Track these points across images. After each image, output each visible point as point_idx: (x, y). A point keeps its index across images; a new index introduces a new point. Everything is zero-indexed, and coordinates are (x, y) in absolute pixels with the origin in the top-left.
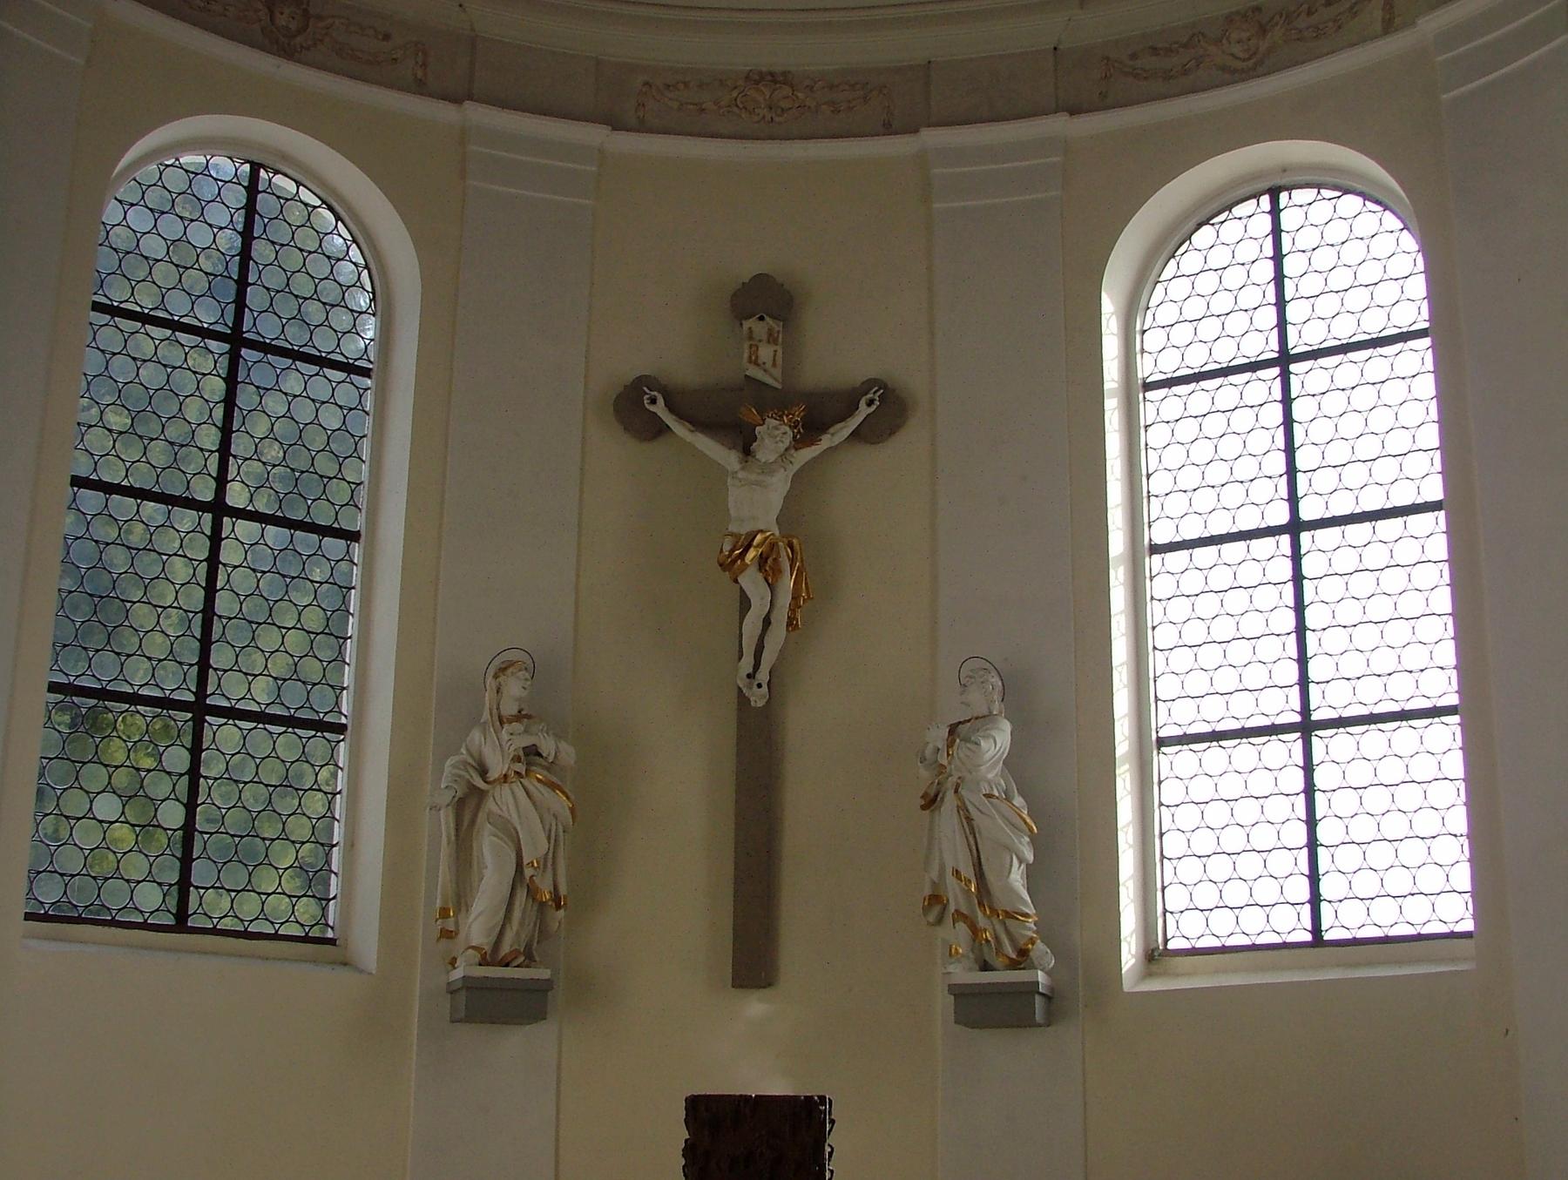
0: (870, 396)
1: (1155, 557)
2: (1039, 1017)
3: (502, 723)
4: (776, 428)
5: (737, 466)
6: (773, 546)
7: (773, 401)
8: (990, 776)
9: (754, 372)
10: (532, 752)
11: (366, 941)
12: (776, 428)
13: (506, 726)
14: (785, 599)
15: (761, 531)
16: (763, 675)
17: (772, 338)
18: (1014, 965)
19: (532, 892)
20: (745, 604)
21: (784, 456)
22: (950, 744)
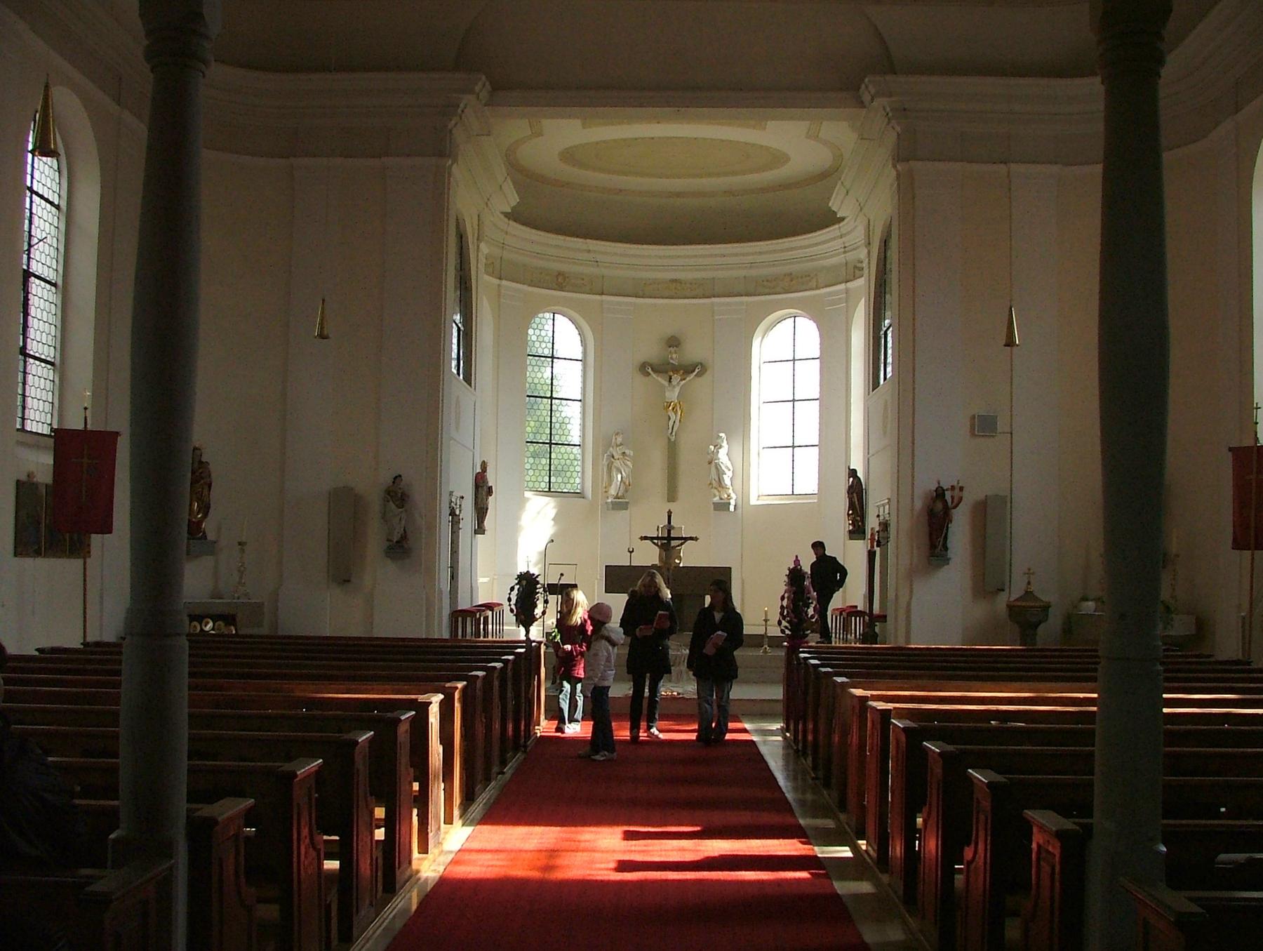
6: (676, 405)
7: (675, 369)
9: (671, 361)
10: (624, 453)
11: (589, 492)
16: (674, 434)
17: (676, 353)
19: (625, 483)
21: (678, 383)
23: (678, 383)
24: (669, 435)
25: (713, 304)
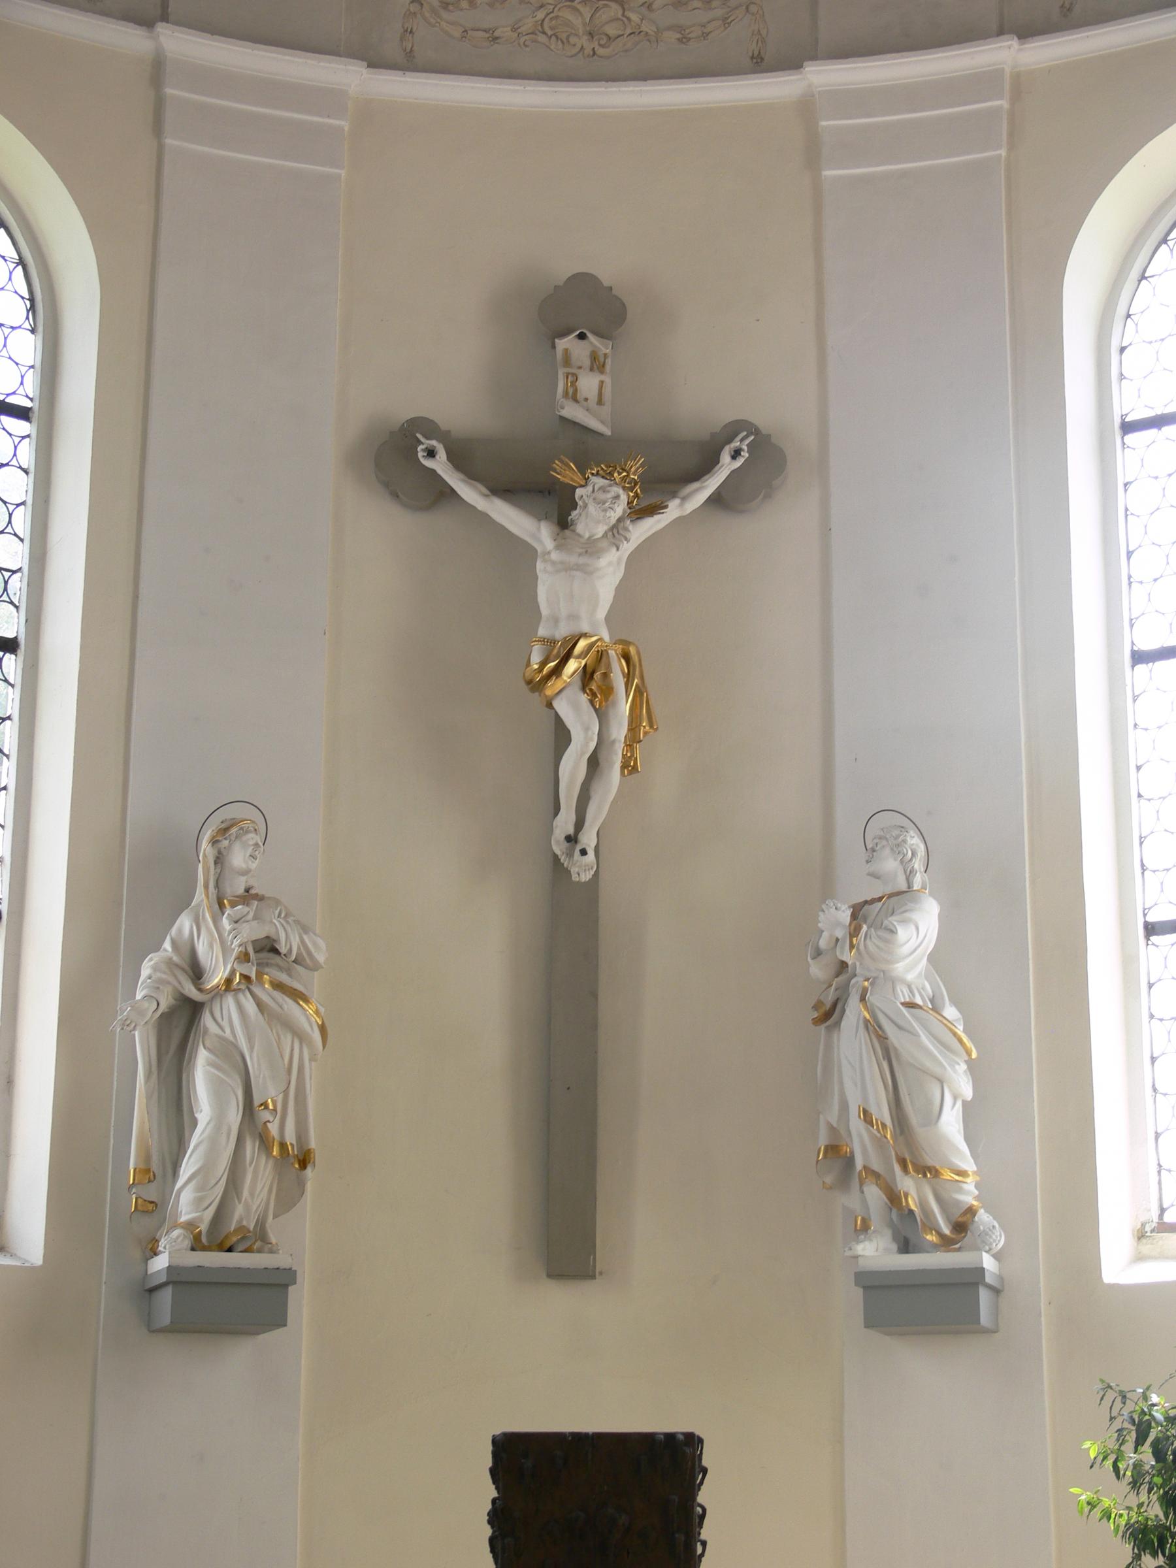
0: (736, 444)
1: (1141, 668)
2: (985, 1318)
3: (221, 906)
4: (603, 489)
5: (549, 544)
6: (601, 656)
8: (910, 977)
9: (571, 411)
10: (269, 947)
12: (603, 489)
13: (228, 911)
14: (619, 731)
15: (585, 635)
16: (589, 839)
17: (597, 364)
18: (947, 1243)
20: (562, 736)
21: (616, 532)
22: (854, 932)
23: (616, 532)
24: (559, 847)
25: (806, 108)
